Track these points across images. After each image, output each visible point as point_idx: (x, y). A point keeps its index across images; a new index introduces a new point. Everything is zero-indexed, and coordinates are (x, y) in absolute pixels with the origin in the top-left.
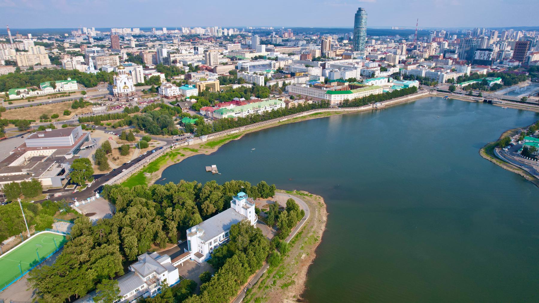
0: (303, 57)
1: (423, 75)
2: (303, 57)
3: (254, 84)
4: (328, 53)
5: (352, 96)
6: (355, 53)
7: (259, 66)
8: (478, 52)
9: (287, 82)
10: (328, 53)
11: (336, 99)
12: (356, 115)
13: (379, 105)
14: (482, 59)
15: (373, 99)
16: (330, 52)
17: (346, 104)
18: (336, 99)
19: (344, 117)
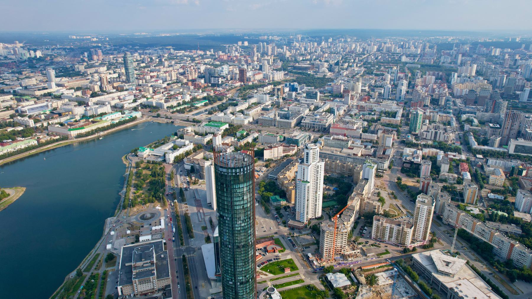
0: (83, 93)
1: (154, 105)
2: (83, 93)
3: (26, 126)
4: (106, 87)
5: (83, 131)
6: (126, 85)
7: (37, 108)
8: (212, 78)
9: (50, 122)
10: (106, 87)
11: (74, 133)
12: (88, 141)
13: (102, 133)
14: (215, 83)
15: (104, 129)
16: (107, 86)
17: (79, 136)
18: (74, 133)
19: (81, 143)
